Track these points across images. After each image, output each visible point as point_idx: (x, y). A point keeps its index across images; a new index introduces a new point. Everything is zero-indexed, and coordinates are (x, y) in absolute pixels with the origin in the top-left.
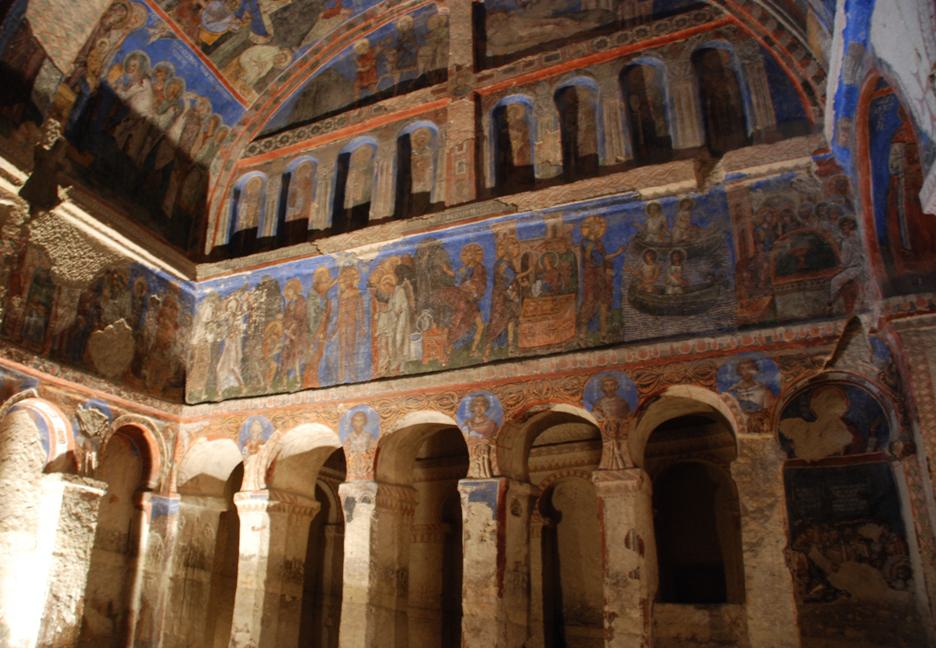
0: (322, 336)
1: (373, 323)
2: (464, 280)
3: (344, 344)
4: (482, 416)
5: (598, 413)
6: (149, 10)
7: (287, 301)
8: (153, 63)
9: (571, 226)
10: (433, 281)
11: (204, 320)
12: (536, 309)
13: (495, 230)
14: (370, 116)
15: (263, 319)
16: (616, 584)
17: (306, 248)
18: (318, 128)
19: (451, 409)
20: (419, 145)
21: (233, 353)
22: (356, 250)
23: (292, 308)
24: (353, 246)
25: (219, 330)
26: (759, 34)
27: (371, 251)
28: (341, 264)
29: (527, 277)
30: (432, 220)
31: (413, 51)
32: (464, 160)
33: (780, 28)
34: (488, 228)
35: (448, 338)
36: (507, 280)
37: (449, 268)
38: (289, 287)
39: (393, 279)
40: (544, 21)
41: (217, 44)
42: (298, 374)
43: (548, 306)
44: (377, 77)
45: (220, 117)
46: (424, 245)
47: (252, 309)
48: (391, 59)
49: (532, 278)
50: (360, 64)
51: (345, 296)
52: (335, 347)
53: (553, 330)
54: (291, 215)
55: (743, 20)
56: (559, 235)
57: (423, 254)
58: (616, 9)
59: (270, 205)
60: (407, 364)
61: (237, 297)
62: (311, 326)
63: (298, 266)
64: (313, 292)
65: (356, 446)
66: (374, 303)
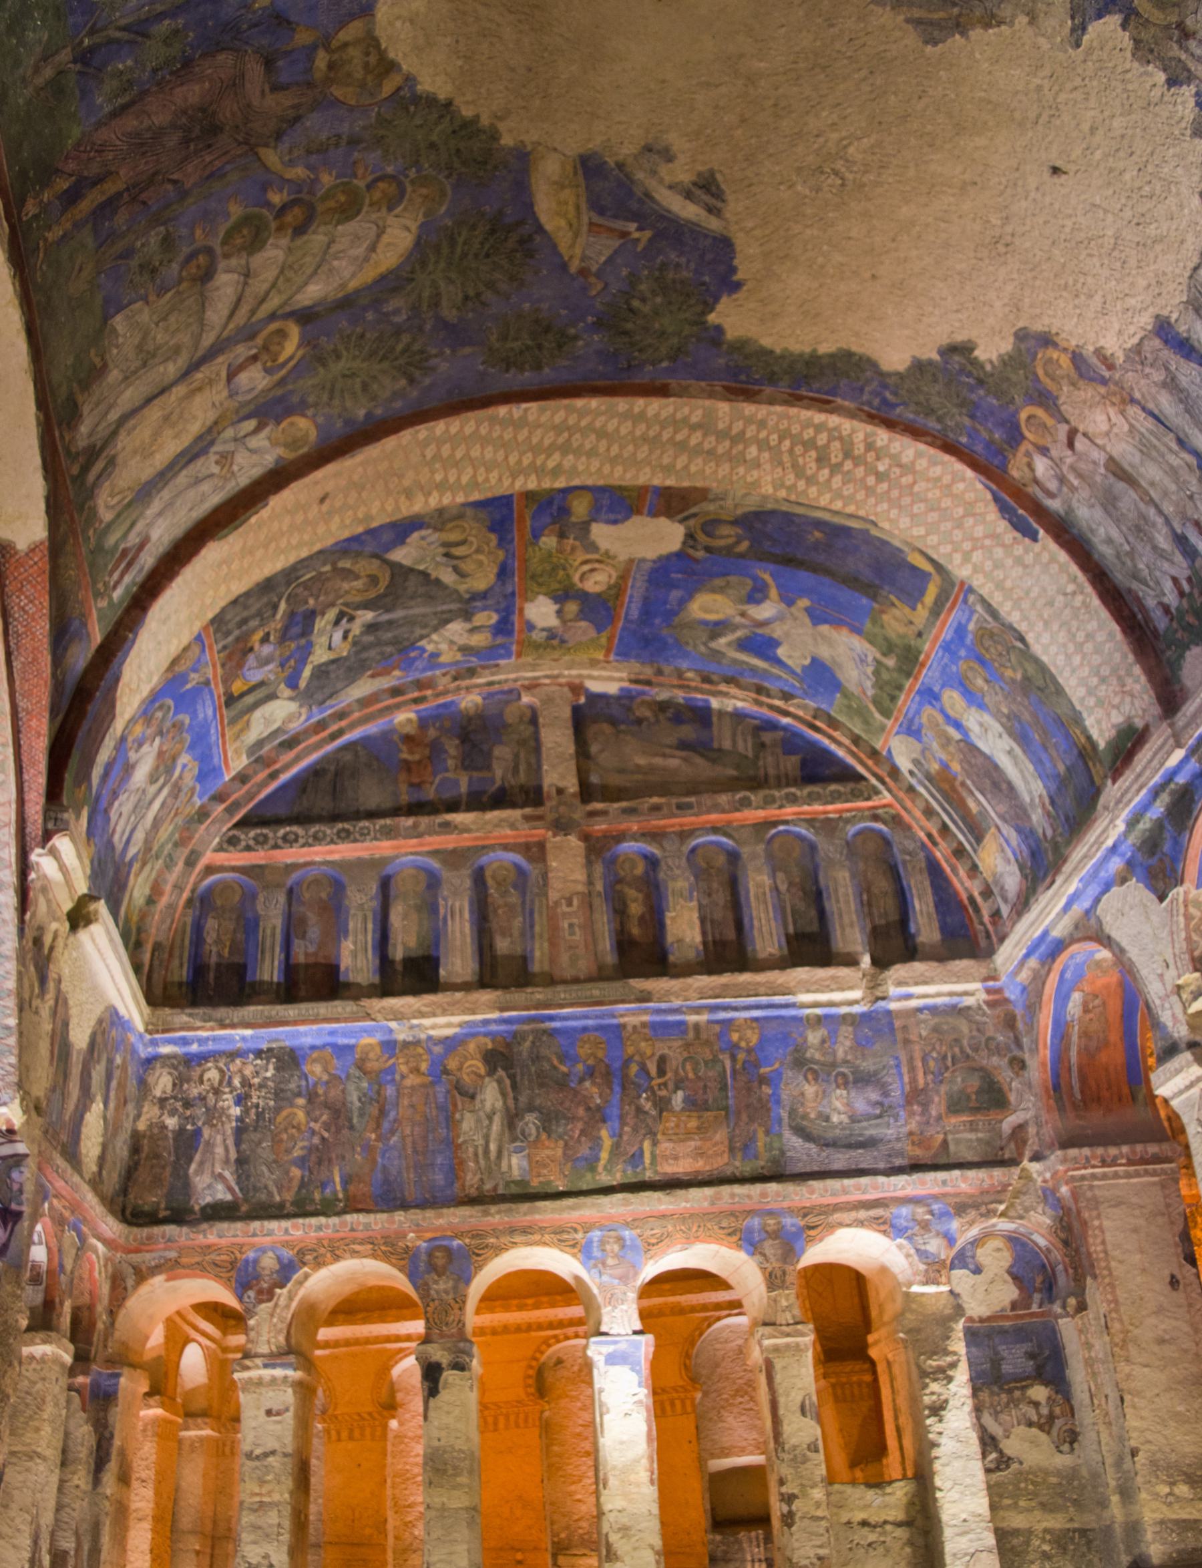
0: (373, 1136)
1: (451, 1123)
2: (582, 1080)
3: (409, 1151)
4: (616, 1256)
5: (761, 1259)
6: (203, 651)
7: (311, 1079)
8: (175, 713)
9: (717, 1028)
10: (538, 1076)
11: (158, 1093)
12: (677, 1126)
13: (622, 1020)
14: (430, 832)
15: (272, 1103)
16: (794, 1459)
17: (348, 1009)
18: (348, 832)
19: (574, 1246)
20: (499, 884)
21: (219, 1150)
22: (427, 1022)
23: (321, 1091)
24: (423, 1015)
25: (188, 1113)
26: (922, 828)
27: (449, 1025)
28: (401, 1037)
29: (665, 1084)
30: (538, 996)
31: (485, 747)
32: (575, 921)
33: (944, 829)
34: (614, 1016)
35: (564, 1154)
36: (639, 1086)
37: (561, 1061)
38: (314, 1061)
39: (482, 1069)
40: (668, 751)
41: (242, 695)
42: (339, 1188)
43: (693, 1124)
44: (435, 774)
45: (198, 787)
46: (526, 1027)
47: (250, 1086)
48: (452, 751)
49: (671, 1086)
50: (404, 748)
51: (408, 1082)
52: (396, 1153)
53: (699, 1153)
54: (302, 952)
55: (905, 809)
56: (704, 1036)
57: (524, 1039)
58: (757, 757)
59: (268, 932)
60: (507, 1184)
61: (221, 1065)
62: (355, 1121)
63: (332, 1033)
64: (353, 1071)
65: (437, 1292)
66: (453, 1097)
